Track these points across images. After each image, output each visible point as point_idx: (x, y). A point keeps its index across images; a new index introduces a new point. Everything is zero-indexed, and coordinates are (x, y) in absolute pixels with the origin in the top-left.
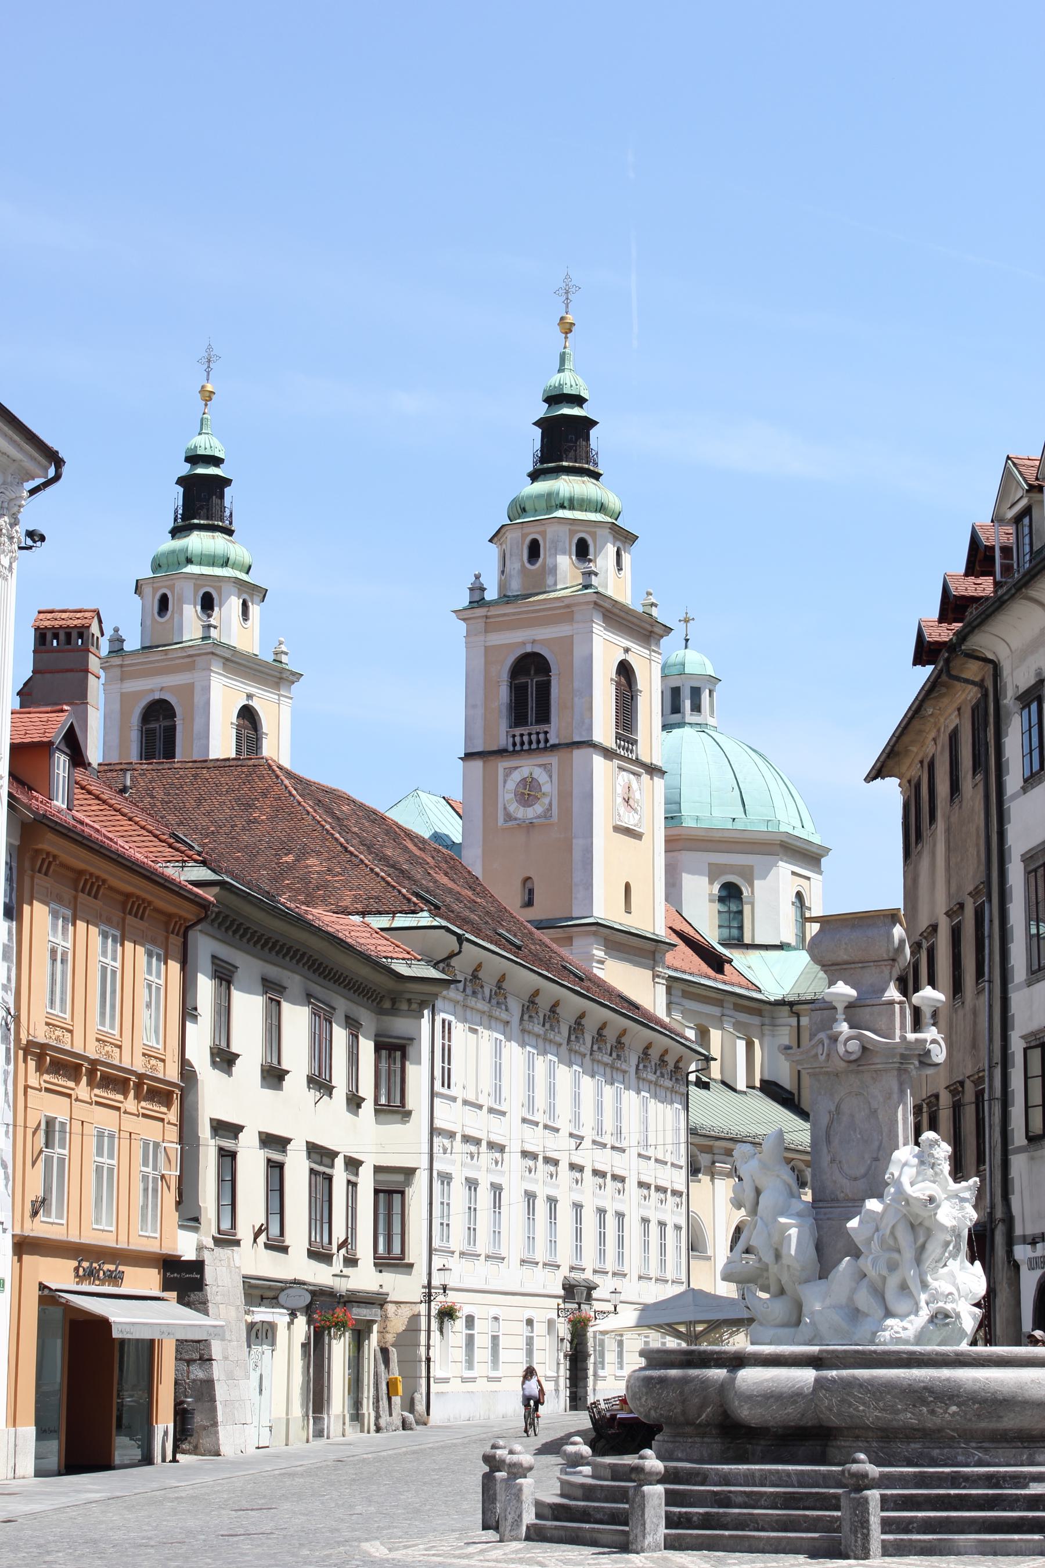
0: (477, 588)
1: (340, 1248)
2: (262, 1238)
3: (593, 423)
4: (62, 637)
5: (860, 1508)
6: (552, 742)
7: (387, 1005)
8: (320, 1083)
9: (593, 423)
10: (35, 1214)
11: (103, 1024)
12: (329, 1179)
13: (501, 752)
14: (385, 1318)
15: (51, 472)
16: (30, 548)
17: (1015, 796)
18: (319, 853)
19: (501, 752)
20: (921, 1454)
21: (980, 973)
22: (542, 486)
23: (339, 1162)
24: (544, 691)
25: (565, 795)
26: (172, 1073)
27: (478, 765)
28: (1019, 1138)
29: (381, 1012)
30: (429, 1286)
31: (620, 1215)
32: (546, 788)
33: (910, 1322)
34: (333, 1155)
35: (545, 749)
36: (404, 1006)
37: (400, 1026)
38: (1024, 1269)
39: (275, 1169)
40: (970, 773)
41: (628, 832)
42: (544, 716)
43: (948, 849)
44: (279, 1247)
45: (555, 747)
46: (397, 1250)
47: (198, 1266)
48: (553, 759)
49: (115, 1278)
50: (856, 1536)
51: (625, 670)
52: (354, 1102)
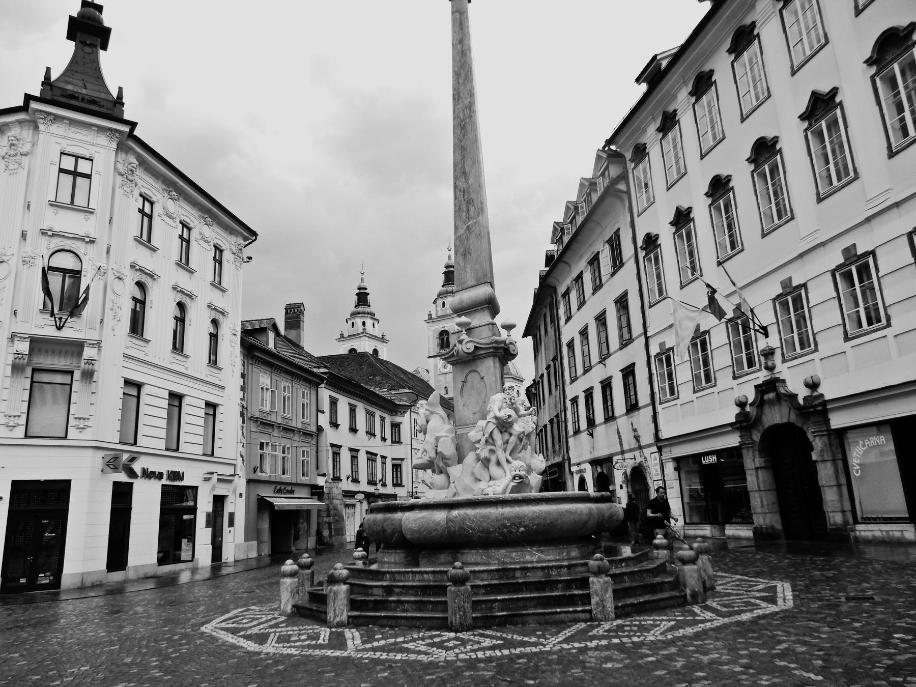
0: (430, 315)
1: (380, 481)
4: (293, 311)
5: (458, 598)
7: (394, 413)
8: (371, 433)
10: (255, 472)
11: (284, 412)
15: (254, 238)
17: (563, 326)
18: (379, 375)
20: (505, 555)
22: (444, 289)
26: (313, 429)
27: (432, 359)
28: (571, 432)
30: (412, 492)
33: (501, 482)
34: (376, 455)
36: (399, 414)
37: (398, 419)
38: (574, 474)
39: (354, 458)
43: (545, 350)
44: (356, 481)
46: (399, 482)
49: (292, 492)
50: (456, 617)
52: (384, 439)
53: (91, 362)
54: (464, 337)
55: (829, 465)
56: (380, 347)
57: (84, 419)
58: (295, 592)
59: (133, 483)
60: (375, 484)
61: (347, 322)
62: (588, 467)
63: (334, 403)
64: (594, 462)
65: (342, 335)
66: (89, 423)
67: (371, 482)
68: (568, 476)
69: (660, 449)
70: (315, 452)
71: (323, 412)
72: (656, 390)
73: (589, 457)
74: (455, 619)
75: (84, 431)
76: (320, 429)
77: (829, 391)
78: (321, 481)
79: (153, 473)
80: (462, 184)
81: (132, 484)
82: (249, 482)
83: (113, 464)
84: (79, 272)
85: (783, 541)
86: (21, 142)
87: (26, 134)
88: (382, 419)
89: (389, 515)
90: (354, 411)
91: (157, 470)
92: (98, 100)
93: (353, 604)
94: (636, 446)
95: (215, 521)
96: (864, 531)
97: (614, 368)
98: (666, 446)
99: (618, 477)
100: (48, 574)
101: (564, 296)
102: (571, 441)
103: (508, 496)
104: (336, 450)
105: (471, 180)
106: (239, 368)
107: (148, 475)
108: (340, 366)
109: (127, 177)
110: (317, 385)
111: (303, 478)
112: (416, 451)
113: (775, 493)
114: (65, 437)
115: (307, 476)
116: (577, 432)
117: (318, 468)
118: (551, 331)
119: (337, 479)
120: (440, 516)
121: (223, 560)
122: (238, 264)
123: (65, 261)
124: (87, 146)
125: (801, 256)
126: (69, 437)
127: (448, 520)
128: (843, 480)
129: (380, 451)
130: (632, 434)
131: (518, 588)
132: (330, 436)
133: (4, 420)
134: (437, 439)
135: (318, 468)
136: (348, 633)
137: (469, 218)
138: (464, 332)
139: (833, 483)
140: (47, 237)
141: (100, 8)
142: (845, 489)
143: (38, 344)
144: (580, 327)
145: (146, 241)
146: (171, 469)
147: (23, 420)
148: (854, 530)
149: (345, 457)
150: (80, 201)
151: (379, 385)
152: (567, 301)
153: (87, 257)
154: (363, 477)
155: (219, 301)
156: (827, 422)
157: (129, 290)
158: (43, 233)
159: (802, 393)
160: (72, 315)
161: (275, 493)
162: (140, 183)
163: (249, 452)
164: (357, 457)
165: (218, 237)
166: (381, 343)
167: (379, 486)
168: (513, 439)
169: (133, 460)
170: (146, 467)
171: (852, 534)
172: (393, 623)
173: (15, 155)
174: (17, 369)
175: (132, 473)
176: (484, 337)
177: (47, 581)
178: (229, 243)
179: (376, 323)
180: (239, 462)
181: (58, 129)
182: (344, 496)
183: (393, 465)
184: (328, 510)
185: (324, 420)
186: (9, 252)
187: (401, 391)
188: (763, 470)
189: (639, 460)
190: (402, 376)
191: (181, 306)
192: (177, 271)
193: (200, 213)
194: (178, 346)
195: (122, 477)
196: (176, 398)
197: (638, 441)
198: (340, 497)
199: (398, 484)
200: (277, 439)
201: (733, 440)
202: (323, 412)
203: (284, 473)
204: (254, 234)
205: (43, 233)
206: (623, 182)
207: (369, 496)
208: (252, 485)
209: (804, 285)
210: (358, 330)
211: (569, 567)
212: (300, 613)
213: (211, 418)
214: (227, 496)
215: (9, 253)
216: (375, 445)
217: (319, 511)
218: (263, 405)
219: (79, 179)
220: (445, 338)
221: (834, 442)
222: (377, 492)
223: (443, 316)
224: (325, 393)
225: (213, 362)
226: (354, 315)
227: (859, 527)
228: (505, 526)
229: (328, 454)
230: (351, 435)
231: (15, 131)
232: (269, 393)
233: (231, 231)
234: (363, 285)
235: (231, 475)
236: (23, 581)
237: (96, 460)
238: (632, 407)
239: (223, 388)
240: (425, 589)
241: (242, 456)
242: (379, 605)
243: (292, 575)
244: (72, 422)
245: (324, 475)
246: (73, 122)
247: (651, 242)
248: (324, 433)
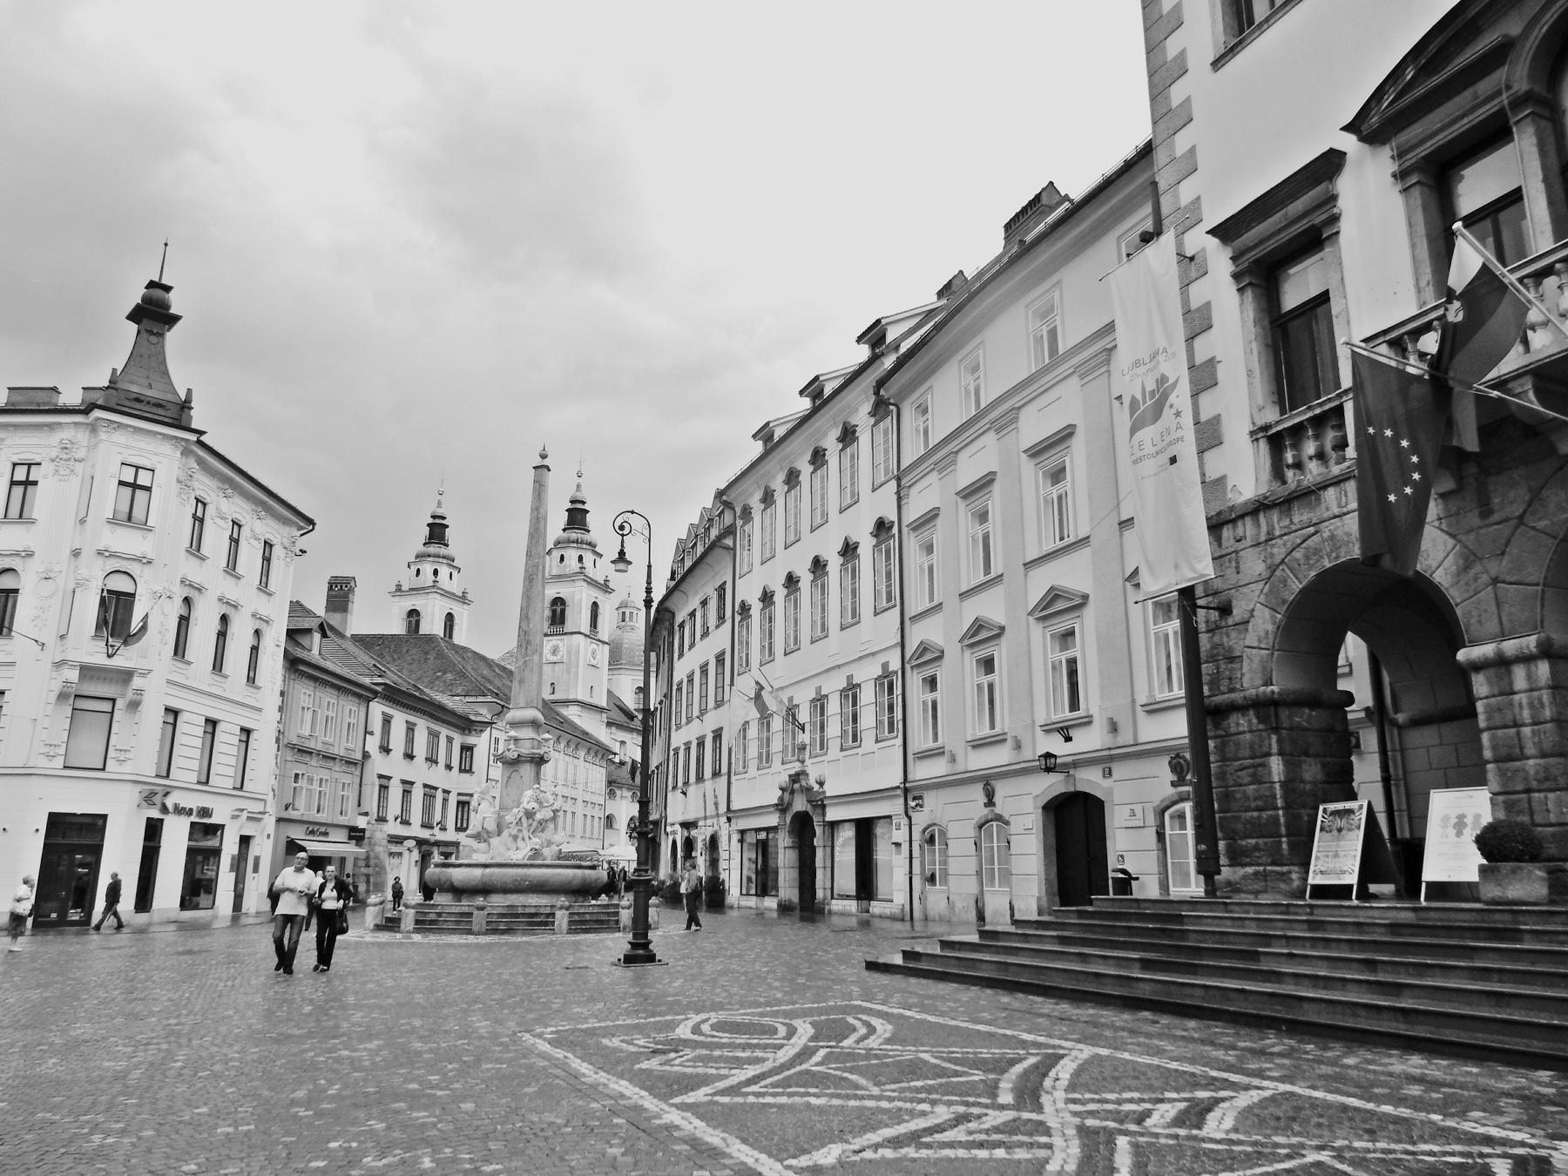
2: (399, 820)
3: (588, 512)
9: (588, 512)
10: (286, 809)
14: (458, 852)
22: (566, 535)
23: (440, 791)
24: (563, 611)
28: (670, 788)
31: (574, 813)
34: (436, 789)
37: (471, 740)
39: (407, 793)
42: (562, 622)
44: (406, 823)
46: (465, 825)
47: (363, 831)
49: (326, 834)
51: (595, 605)
52: (449, 767)
53: (139, 692)
54: (512, 747)
55: (821, 849)
56: (458, 610)
57: (126, 751)
58: (375, 917)
59: (162, 820)
60: (432, 828)
61: (409, 567)
62: (678, 827)
63: (387, 721)
64: (687, 825)
65: (399, 588)
66: (129, 755)
68: (663, 836)
69: (729, 820)
70: (357, 786)
71: (371, 733)
72: (733, 760)
73: (681, 818)
74: (475, 928)
75: (124, 763)
76: (366, 755)
77: (831, 790)
78: (361, 822)
79: (184, 809)
80: (524, 625)
81: (162, 820)
82: (279, 820)
83: (149, 799)
84: (133, 595)
85: (797, 912)
86: (76, 446)
87: (82, 437)
88: (450, 740)
89: (444, 869)
90: (413, 730)
91: (188, 806)
92: (164, 403)
93: (417, 922)
94: (714, 813)
95: (239, 864)
96: (837, 905)
97: (706, 727)
98: (737, 817)
99: (700, 845)
100: (79, 910)
102: (669, 795)
103: (525, 862)
104: (384, 782)
105: (531, 626)
106: (278, 686)
107: (179, 811)
108: (395, 651)
109: (184, 484)
110: (369, 700)
111: (341, 818)
113: (797, 870)
114: (104, 769)
115: (346, 815)
116: (674, 788)
117: (359, 805)
118: (666, 659)
119: (382, 819)
120: (478, 872)
121: (244, 910)
122: (288, 560)
123: (121, 584)
124: (148, 455)
125: (827, 671)
126: (107, 769)
127: (483, 875)
128: (829, 864)
130: (713, 800)
131: (517, 915)
132: (379, 764)
133: (46, 749)
134: (484, 818)
135: (359, 805)
136: (413, 935)
137: (526, 654)
138: (512, 742)
139: (821, 865)
140: (103, 558)
141: (168, 289)
142: (829, 870)
143: (87, 671)
144: (688, 671)
145: (195, 547)
146: (201, 805)
147: (62, 751)
148: (828, 904)
149: (395, 792)
150: (138, 514)
151: (449, 689)
153: (143, 580)
154: (416, 816)
155: (264, 606)
156: (824, 815)
157: (175, 609)
158: (100, 553)
159: (816, 787)
160: (125, 643)
161: (306, 834)
162: (196, 485)
163: (282, 786)
164: (410, 792)
166: (460, 604)
167: (437, 830)
168: (535, 824)
169: (166, 794)
171: (827, 908)
172: (441, 931)
173: (69, 459)
174: (62, 697)
175: (164, 809)
176: (526, 749)
177: (77, 918)
178: (279, 533)
179: (455, 573)
180: (270, 798)
181: (120, 437)
182: (389, 841)
183: (459, 803)
184: (367, 858)
185: (373, 744)
186: (56, 569)
187: (481, 699)
188: (791, 850)
189: (716, 827)
190: (485, 672)
191: (224, 619)
193: (254, 507)
194: (218, 665)
195: (155, 814)
196: (212, 723)
197: (717, 809)
198: (385, 842)
200: (319, 772)
201: (772, 820)
202: (371, 733)
203: (318, 811)
204: (311, 522)
205: (100, 553)
206: (731, 537)
207: (421, 842)
208: (282, 824)
209: (827, 696)
210: (425, 582)
211: (552, 906)
212: (378, 928)
213: (244, 745)
215: (56, 569)
216: (436, 776)
217: (356, 859)
218: (301, 729)
219: (138, 492)
220: (559, 611)
221: (827, 833)
222: (433, 839)
223: (559, 576)
224: (378, 708)
225: (251, 680)
226: (421, 557)
227: (834, 902)
228: (517, 880)
230: (406, 762)
231: (66, 434)
232: (310, 712)
233: (285, 521)
234: (440, 512)
235: (260, 813)
236: (54, 915)
237: (132, 794)
238: (716, 774)
239: (260, 710)
240: (462, 914)
241: (273, 790)
242: (432, 922)
243: (375, 905)
244: (111, 753)
245: (366, 814)
246: (137, 430)
247: (745, 609)
248: (370, 760)
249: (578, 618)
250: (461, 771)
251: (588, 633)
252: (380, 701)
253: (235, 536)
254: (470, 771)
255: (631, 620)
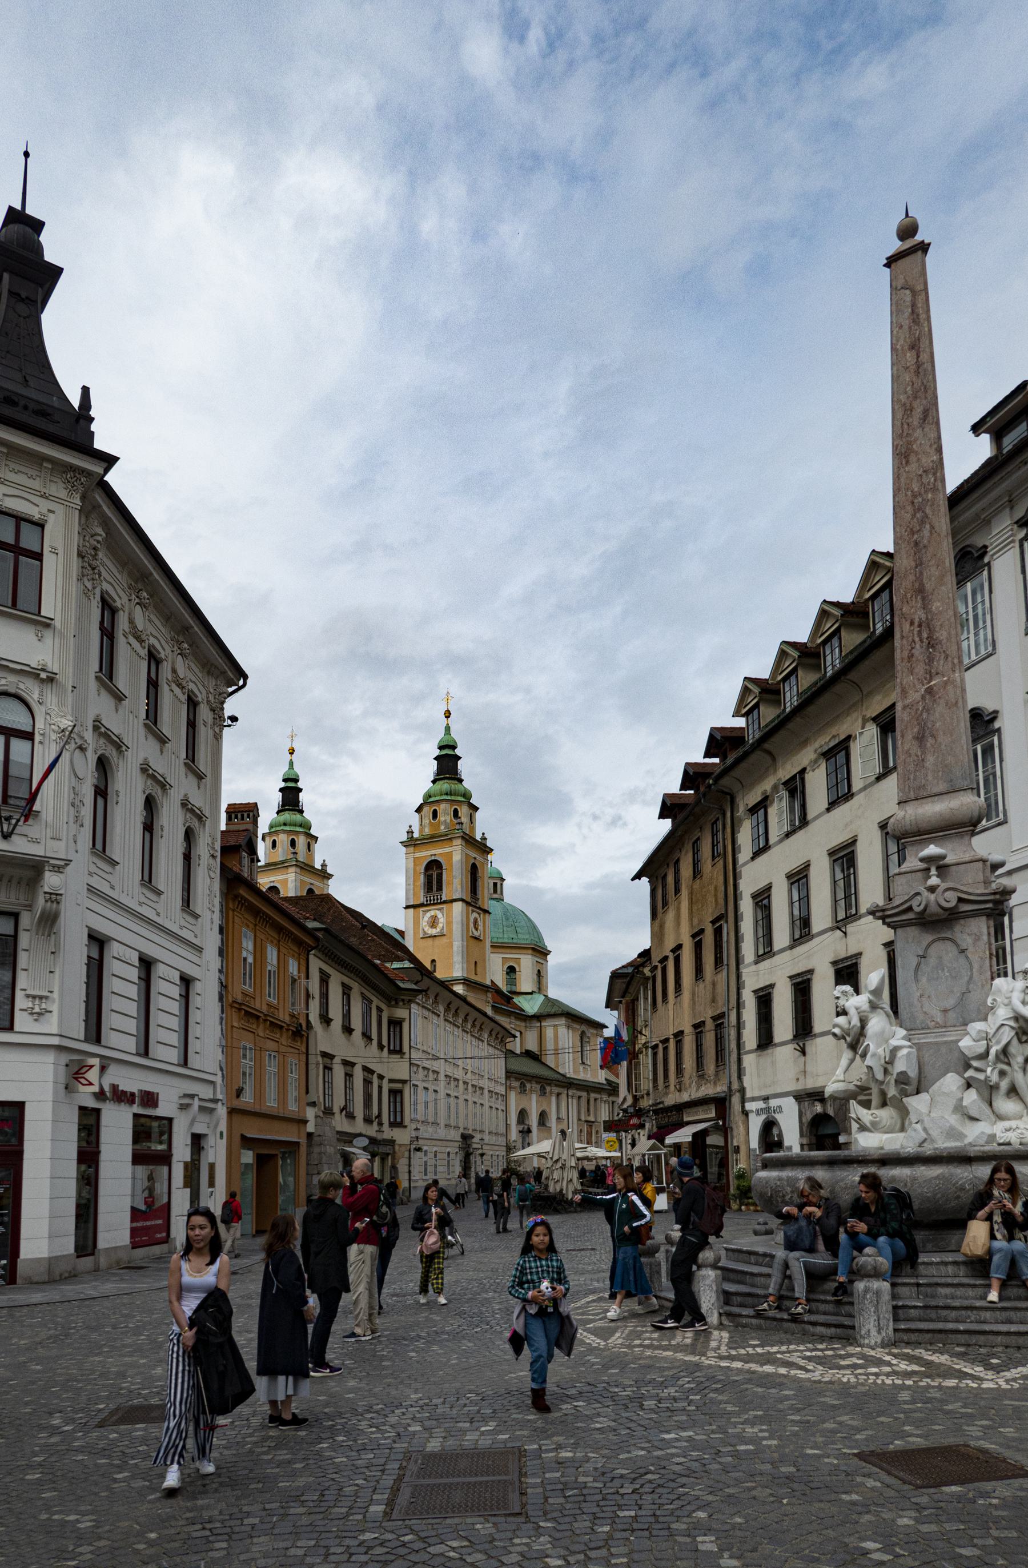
4: (239, 816)
6: (444, 898)
7: (393, 1003)
12: (371, 1083)
13: (422, 905)
14: (394, 1152)
16: (229, 726)
19: (422, 905)
21: (718, 961)
23: (375, 1075)
25: (449, 923)
27: (411, 910)
29: (389, 1006)
32: (441, 920)
34: (372, 1072)
35: (441, 903)
37: (401, 1013)
39: (349, 1076)
40: (710, 858)
41: (476, 938)
42: (440, 888)
44: (351, 1116)
45: (445, 902)
46: (399, 1119)
48: (444, 906)
52: (381, 1047)
63: (325, 979)
67: (368, 1120)
88: (379, 1010)
101: (753, 810)
112: (415, 1069)
119: (328, 1112)
129: (378, 1069)
135: (307, 1092)
152: (761, 818)
154: (359, 1111)
165: (194, 679)
167: (375, 1124)
170: (116, 1083)
182: (338, 1140)
187: (396, 965)
192: (146, 738)
199: (397, 1124)
207: (373, 1141)
214: (206, 1135)
229: (318, 1068)
249: (455, 884)
250: (391, 1052)
251: (469, 900)
252: (319, 955)
253: (153, 675)
254: (400, 1052)
255: (495, 891)
